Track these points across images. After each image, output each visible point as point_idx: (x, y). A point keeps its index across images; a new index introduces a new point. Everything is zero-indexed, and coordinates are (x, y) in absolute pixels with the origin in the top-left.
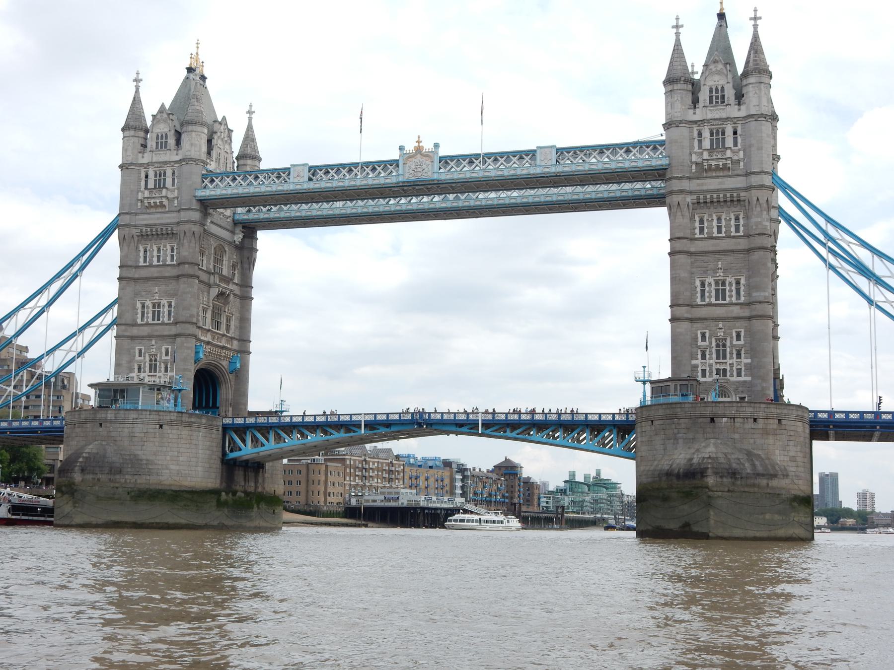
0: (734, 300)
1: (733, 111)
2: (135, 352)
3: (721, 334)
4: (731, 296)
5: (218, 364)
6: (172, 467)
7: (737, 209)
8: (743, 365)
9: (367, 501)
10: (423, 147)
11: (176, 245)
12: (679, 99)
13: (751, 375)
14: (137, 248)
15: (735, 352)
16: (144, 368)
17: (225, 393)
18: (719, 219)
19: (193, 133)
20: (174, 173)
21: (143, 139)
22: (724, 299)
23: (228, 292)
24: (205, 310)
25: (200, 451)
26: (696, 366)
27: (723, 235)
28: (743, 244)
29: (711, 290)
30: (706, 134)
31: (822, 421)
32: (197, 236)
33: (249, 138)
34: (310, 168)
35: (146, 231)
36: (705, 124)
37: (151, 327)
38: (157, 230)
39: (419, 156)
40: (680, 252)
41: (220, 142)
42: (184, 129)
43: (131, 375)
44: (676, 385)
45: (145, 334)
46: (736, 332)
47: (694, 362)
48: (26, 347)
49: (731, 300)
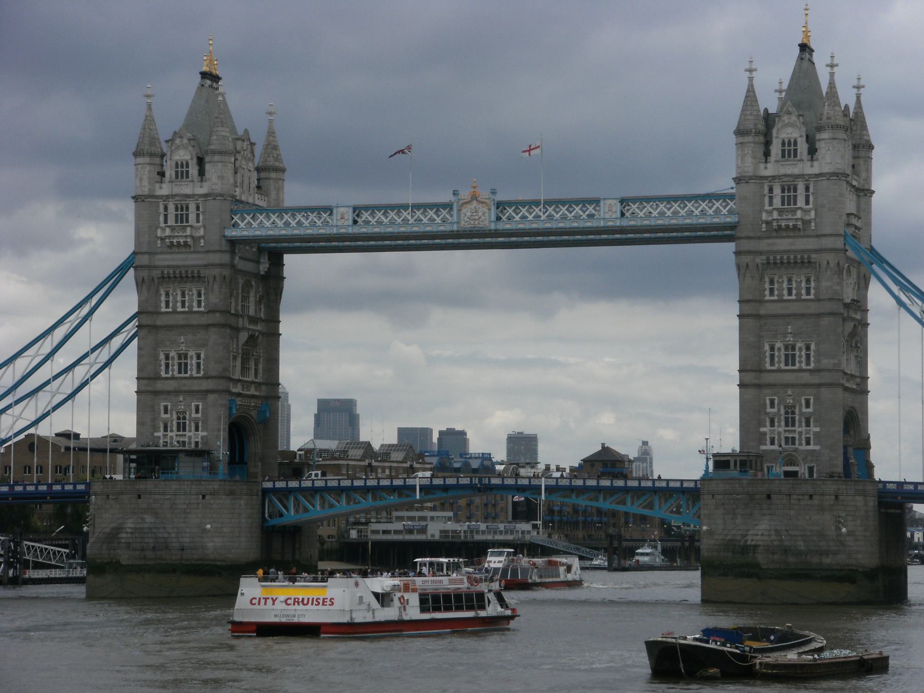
0: (804, 366)
2: (160, 409)
3: (790, 401)
4: (800, 362)
5: (248, 416)
8: (812, 433)
12: (750, 152)
14: (157, 291)
15: (803, 420)
17: (254, 447)
18: (790, 281)
19: (220, 165)
20: (198, 208)
21: (159, 166)
22: (794, 364)
23: (257, 333)
24: (235, 358)
26: (765, 434)
27: (794, 297)
28: (813, 308)
29: (780, 355)
30: (777, 191)
35: (168, 273)
36: (776, 181)
38: (180, 272)
39: (475, 202)
40: (748, 316)
41: (243, 162)
43: (156, 434)
44: (736, 461)
46: (805, 399)
47: (762, 429)
49: (800, 366)
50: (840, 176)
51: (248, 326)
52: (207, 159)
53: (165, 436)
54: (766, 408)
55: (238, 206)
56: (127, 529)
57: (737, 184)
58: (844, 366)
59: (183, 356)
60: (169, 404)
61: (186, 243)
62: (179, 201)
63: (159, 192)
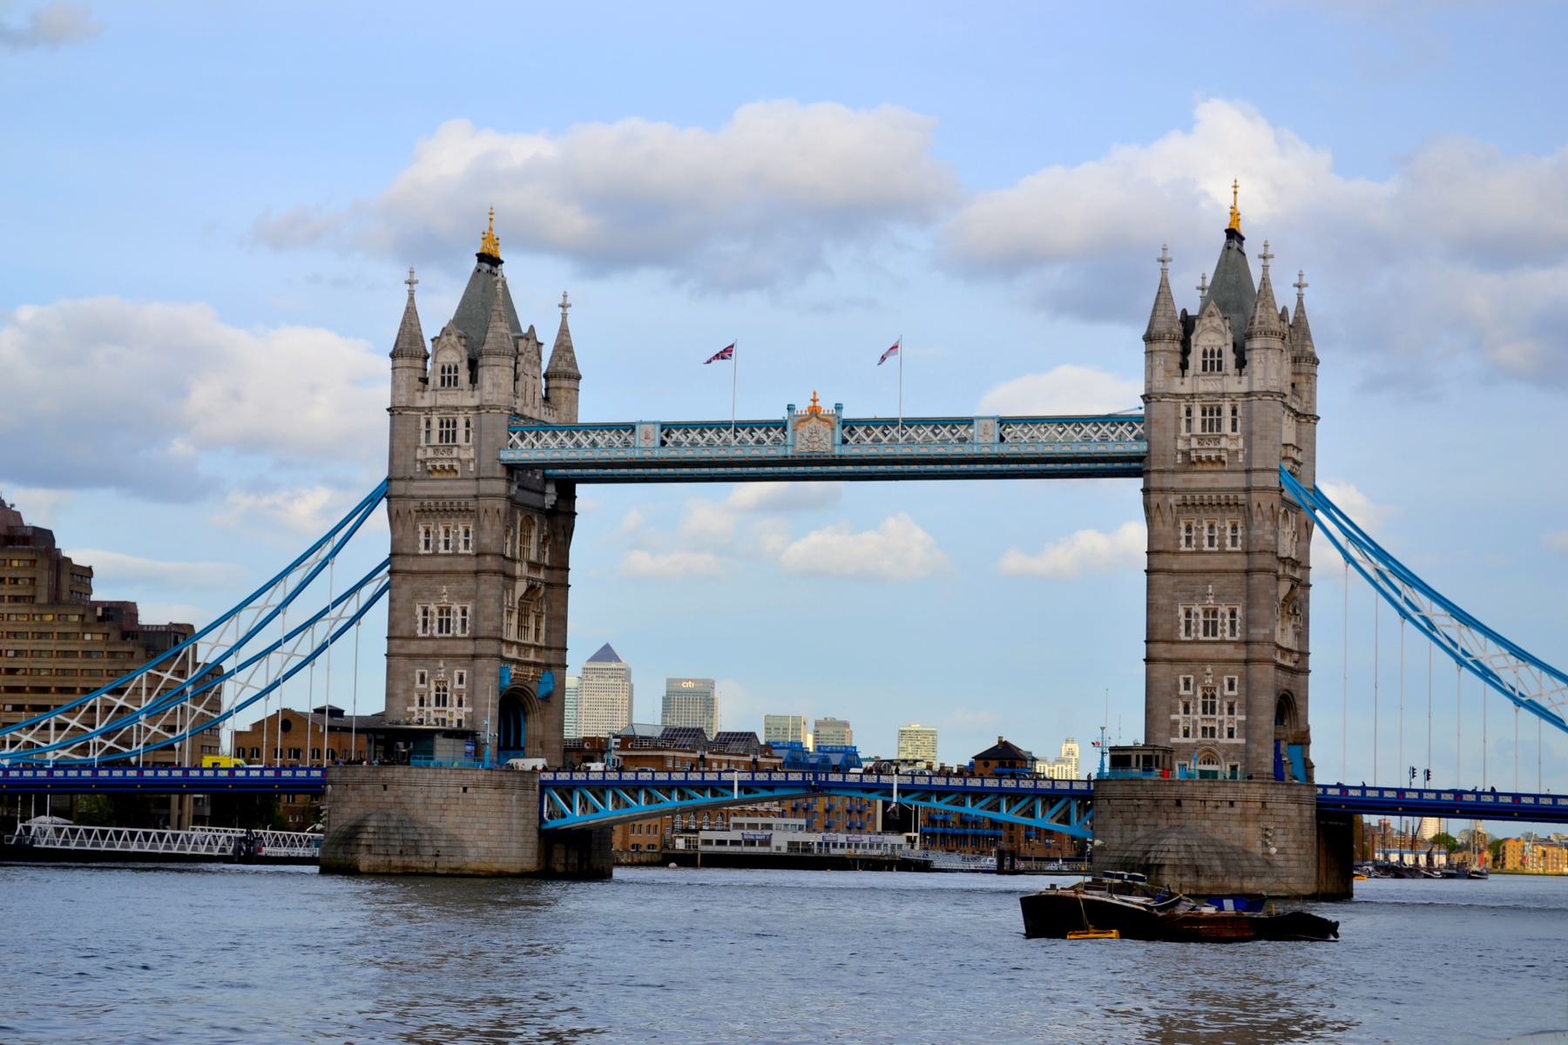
0: (1227, 636)
1: (1233, 384)
3: (1209, 681)
6: (480, 844)
7: (1235, 514)
9: (708, 842)
10: (820, 408)
13: (1247, 736)
14: (415, 528)
15: (1226, 706)
16: (429, 701)
17: (533, 727)
19: (496, 368)
20: (468, 424)
21: (422, 371)
22: (1214, 634)
24: (510, 613)
25: (515, 821)
26: (1176, 723)
30: (1197, 413)
31: (1333, 799)
33: (564, 347)
35: (429, 505)
41: (527, 366)
43: (409, 709)
44: (1138, 757)
45: (429, 651)
47: (1173, 717)
48: (90, 569)
50: (1275, 396)
52: (480, 362)
53: (421, 711)
54: (1178, 690)
55: (519, 422)
57: (1146, 403)
58: (1278, 639)
60: (426, 671)
61: (451, 467)
63: (420, 403)
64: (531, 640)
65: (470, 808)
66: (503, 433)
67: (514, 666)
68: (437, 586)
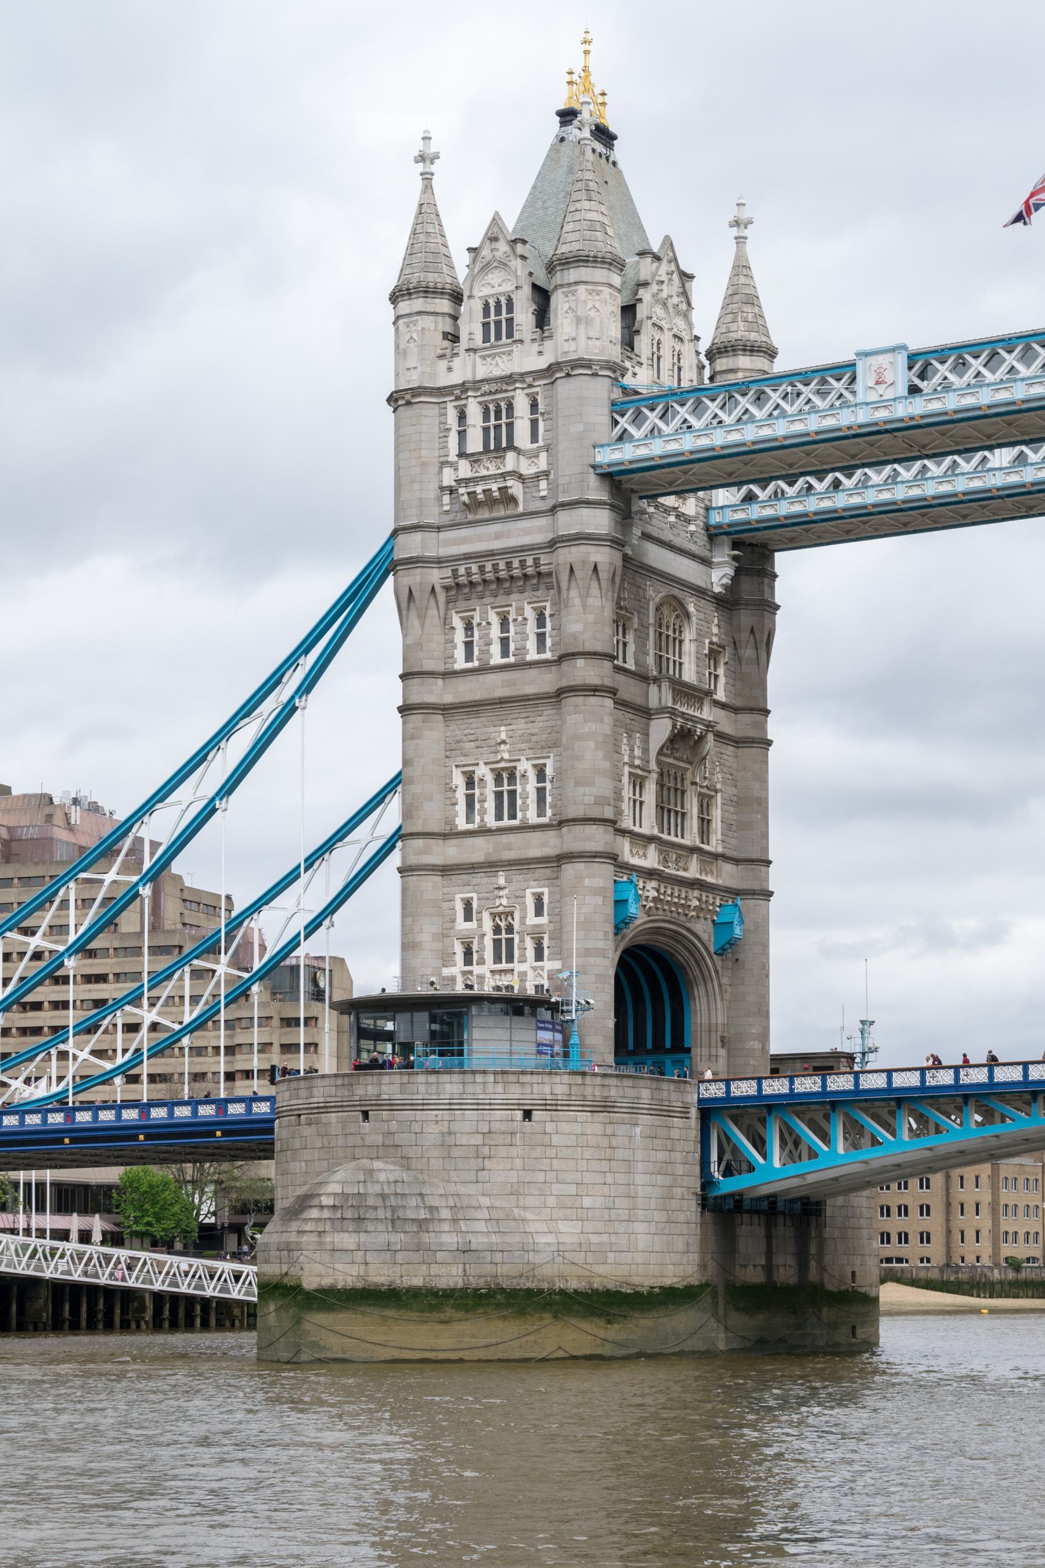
11: (548, 604)
14: (446, 621)
19: (582, 288)
20: (534, 406)
21: (448, 320)
25: (640, 1179)
32: (604, 575)
34: (912, 359)
35: (469, 574)
37: (493, 839)
41: (659, 311)
42: (559, 278)
43: (446, 972)
45: (478, 857)
51: (670, 705)
56: (323, 1198)
59: (505, 775)
60: (474, 895)
62: (491, 393)
64: (691, 837)
65: (538, 1152)
66: (601, 416)
67: (654, 884)
68: (492, 729)
